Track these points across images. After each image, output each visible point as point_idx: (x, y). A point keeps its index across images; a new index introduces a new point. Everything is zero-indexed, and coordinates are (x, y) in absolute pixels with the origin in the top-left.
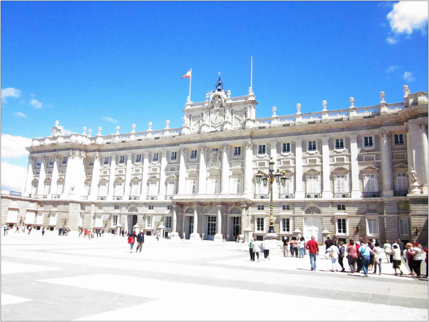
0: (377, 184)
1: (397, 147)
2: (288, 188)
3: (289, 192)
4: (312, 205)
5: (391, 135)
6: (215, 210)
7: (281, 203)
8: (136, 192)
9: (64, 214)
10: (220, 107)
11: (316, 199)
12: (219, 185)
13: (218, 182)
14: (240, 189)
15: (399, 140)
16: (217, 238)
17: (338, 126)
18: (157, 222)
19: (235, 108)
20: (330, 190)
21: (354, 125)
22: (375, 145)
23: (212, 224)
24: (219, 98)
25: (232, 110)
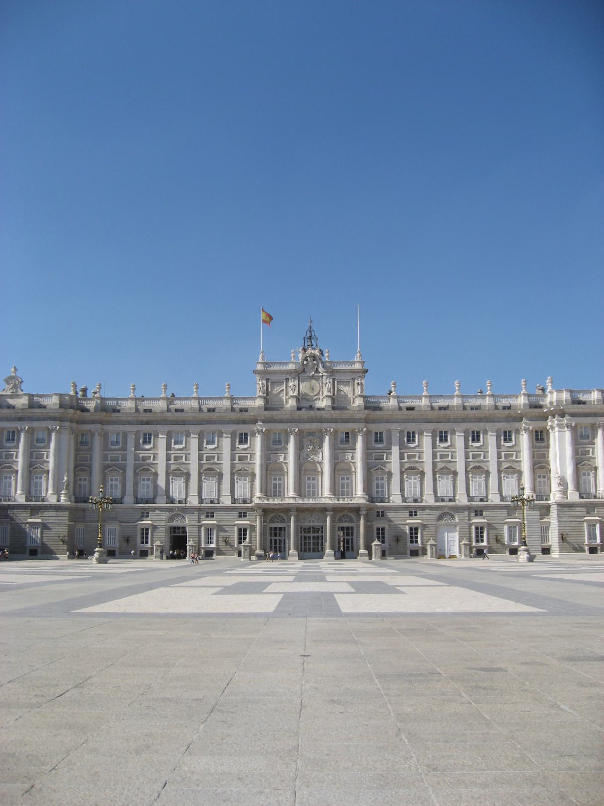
1: (538, 444)
4: (446, 510)
6: (317, 517)
7: (406, 508)
8: (180, 492)
10: (315, 372)
15: (539, 437)
17: (477, 415)
19: (337, 376)
23: (305, 538)
24: (314, 360)
25: (334, 379)
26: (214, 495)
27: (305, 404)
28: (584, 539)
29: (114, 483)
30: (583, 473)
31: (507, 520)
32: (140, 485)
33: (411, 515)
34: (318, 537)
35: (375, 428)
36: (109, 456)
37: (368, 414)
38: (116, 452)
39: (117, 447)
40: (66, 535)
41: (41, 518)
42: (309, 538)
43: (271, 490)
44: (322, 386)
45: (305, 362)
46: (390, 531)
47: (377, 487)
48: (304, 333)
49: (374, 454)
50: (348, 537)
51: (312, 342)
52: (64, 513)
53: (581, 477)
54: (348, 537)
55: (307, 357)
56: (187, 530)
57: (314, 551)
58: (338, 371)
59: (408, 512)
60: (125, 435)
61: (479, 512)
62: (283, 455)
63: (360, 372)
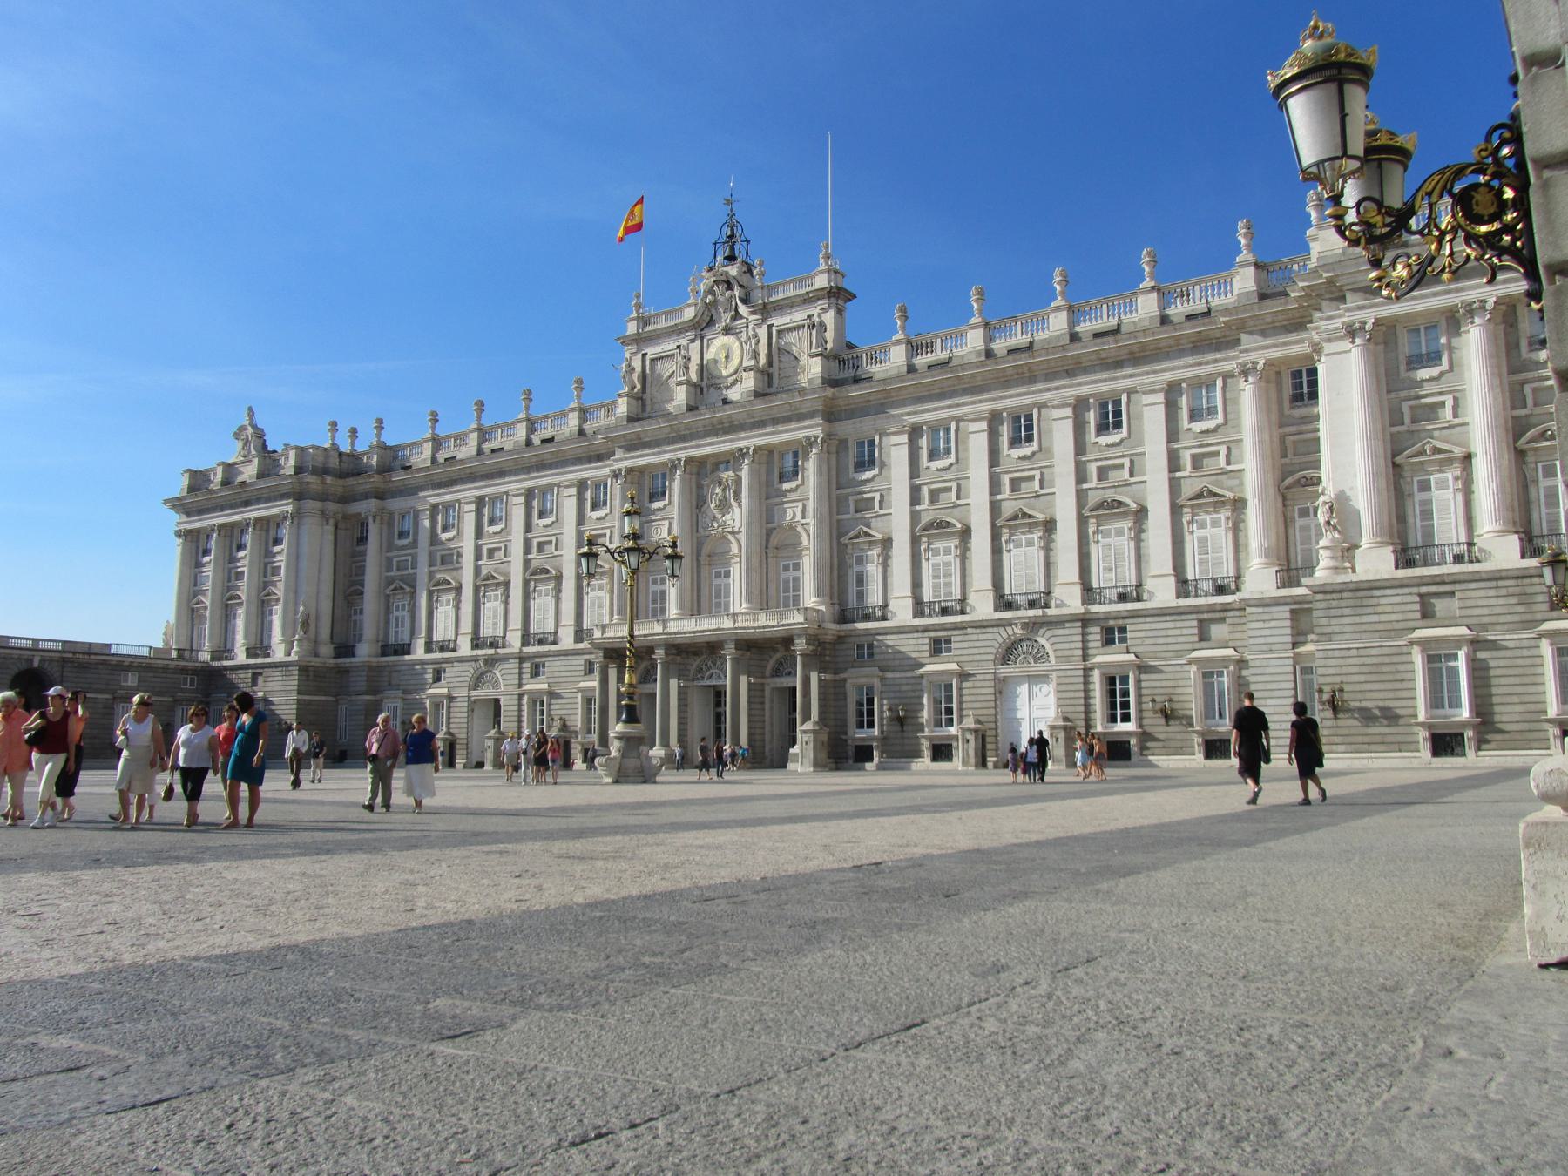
5: (1278, 373)
7: (926, 629)
8: (495, 624)
11: (1032, 613)
15: (1305, 390)
17: (1104, 355)
21: (1152, 347)
26: (549, 627)
28: (1415, 707)
30: (1419, 482)
31: (1196, 654)
36: (395, 560)
43: (647, 607)
45: (709, 298)
48: (713, 230)
51: (732, 248)
53: (1411, 495)
62: (667, 523)
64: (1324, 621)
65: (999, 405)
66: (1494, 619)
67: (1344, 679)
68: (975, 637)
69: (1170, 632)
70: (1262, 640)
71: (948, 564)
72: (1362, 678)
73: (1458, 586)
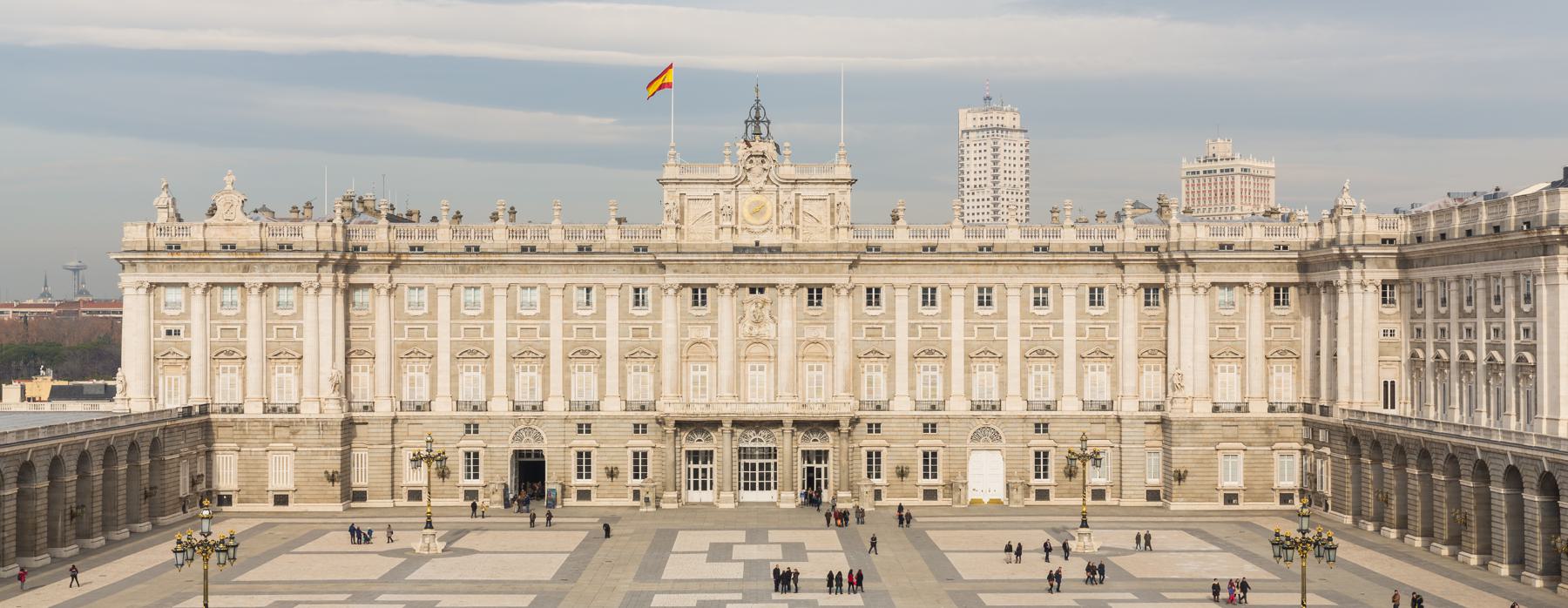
0: (1109, 385)
2: (934, 387)
3: (934, 396)
7: (921, 417)
8: (532, 390)
9: (324, 457)
10: (766, 182)
11: (994, 413)
12: (773, 377)
13: (769, 370)
14: (823, 386)
16: (787, 501)
18: (610, 467)
19: (805, 191)
20: (1019, 393)
22: (1110, 307)
23: (746, 465)
27: (746, 240)
29: (416, 374)
30: (1222, 367)
32: (462, 380)
33: (926, 431)
34: (768, 465)
35: (864, 279)
36: (406, 327)
37: (854, 261)
38: (418, 322)
39: (420, 313)
40: (339, 471)
41: (292, 441)
42: (753, 466)
43: (687, 387)
44: (778, 209)
45: (748, 166)
46: (889, 458)
47: (870, 383)
49: (864, 327)
50: (819, 466)
51: (757, 127)
52: (334, 432)
54: (819, 466)
55: (751, 156)
56: (545, 454)
57: (761, 488)
58: (806, 182)
59: (922, 425)
60: (434, 290)
61: (1043, 428)
63: (843, 183)
64: (1177, 436)
65: (973, 280)
66: (1254, 440)
67: (1186, 465)
68: (953, 425)
69: (1074, 429)
70: (1129, 438)
71: (933, 377)
72: (1193, 465)
73: (1240, 423)
